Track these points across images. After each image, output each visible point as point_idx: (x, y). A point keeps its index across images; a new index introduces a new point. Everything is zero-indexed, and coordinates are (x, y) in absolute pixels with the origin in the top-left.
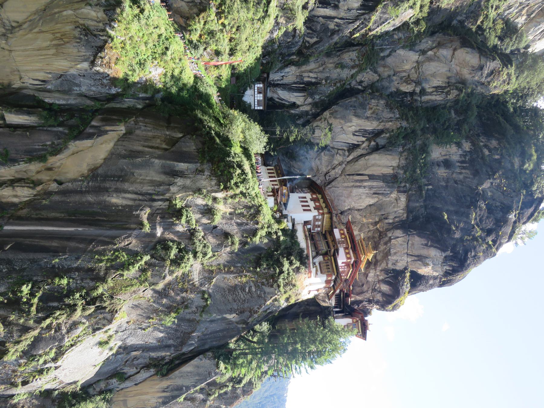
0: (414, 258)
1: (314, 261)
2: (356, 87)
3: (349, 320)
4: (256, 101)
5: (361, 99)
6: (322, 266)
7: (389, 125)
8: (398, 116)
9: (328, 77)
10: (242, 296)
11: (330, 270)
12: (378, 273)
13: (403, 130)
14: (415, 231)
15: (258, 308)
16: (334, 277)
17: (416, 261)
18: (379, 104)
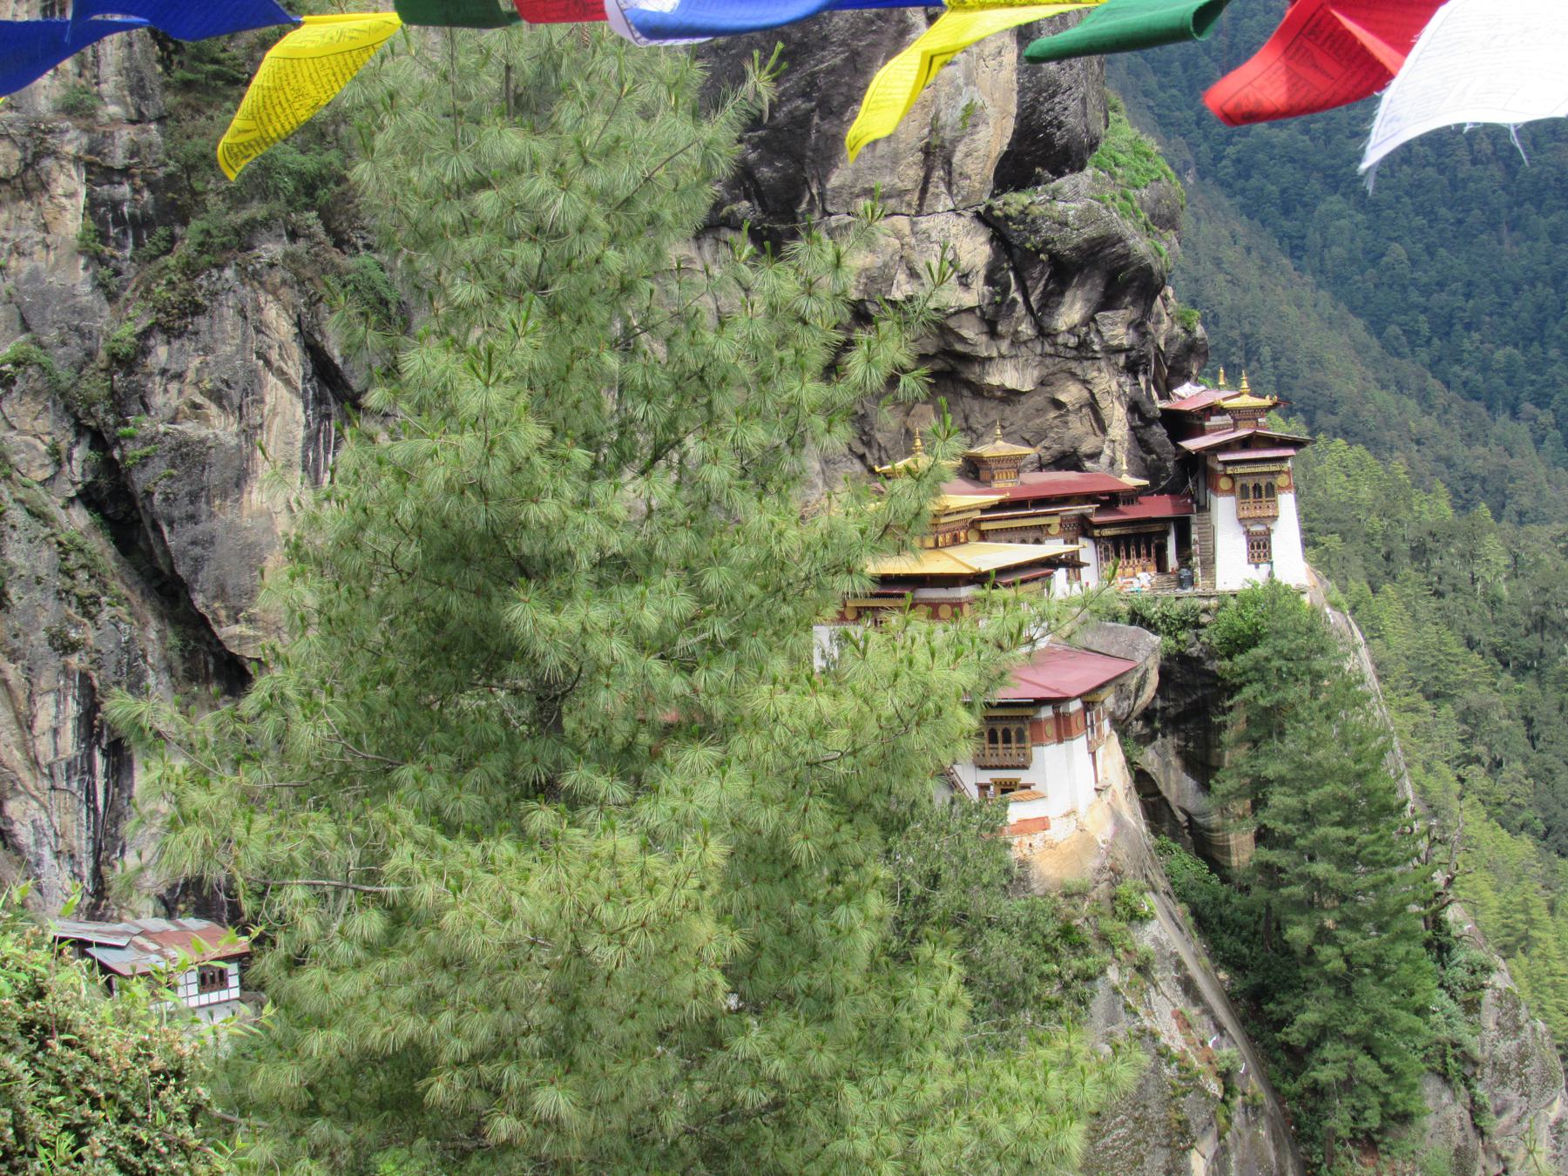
0: (938, 186)
1: (974, 794)
2: (78, 478)
3: (1224, 509)
4: (204, 999)
5: (159, 467)
6: (994, 761)
7: (281, 325)
8: (229, 273)
9: (52, 639)
10: (1122, 1132)
11: (1014, 728)
12: (1004, 346)
13: (302, 245)
14: (806, 182)
15: (1168, 1064)
16: (1046, 713)
17: (950, 173)
18: (174, 368)
